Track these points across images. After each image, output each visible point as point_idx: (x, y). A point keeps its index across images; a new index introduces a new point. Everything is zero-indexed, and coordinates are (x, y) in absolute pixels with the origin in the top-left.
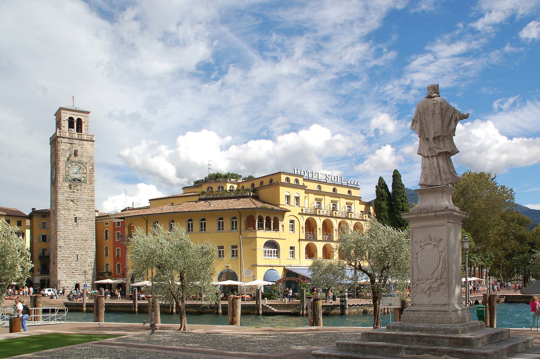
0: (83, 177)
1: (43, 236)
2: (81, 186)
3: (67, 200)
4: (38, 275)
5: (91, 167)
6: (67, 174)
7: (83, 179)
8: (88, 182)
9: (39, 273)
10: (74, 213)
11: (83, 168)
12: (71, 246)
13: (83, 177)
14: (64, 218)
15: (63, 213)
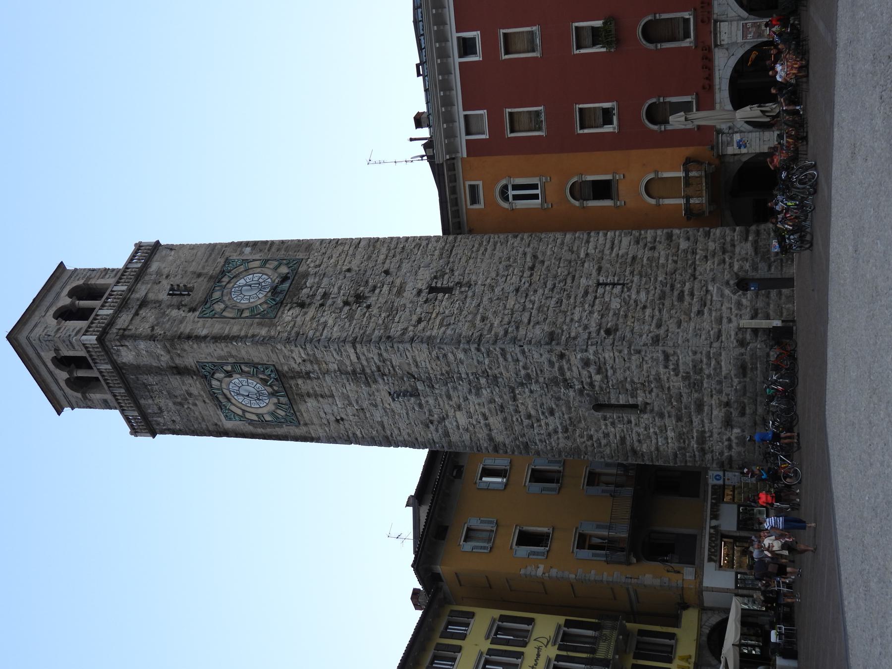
0: (276, 268)
1: (519, 543)
2: (306, 275)
3: (350, 317)
4: (699, 575)
5: (248, 250)
6: (246, 314)
7: (284, 270)
8: (300, 256)
9: (688, 573)
10: (410, 293)
11: (242, 268)
12: (553, 302)
13: (276, 268)
14: (423, 325)
15: (401, 326)
